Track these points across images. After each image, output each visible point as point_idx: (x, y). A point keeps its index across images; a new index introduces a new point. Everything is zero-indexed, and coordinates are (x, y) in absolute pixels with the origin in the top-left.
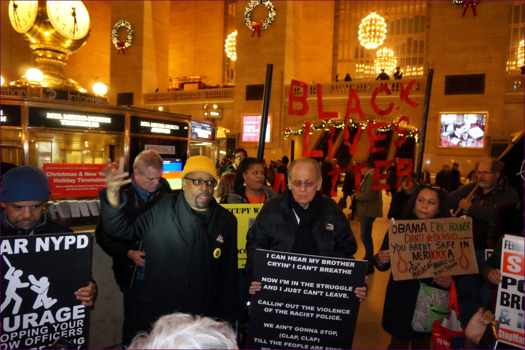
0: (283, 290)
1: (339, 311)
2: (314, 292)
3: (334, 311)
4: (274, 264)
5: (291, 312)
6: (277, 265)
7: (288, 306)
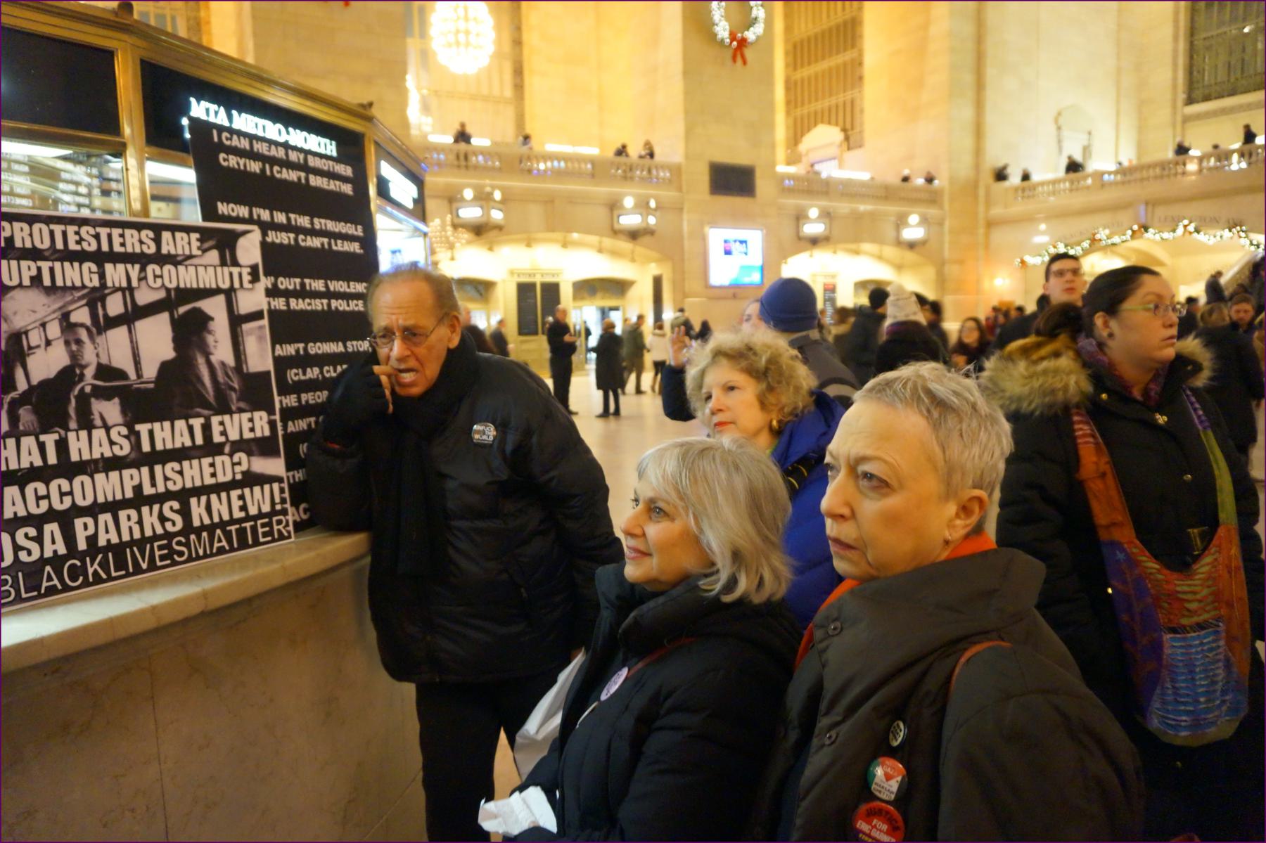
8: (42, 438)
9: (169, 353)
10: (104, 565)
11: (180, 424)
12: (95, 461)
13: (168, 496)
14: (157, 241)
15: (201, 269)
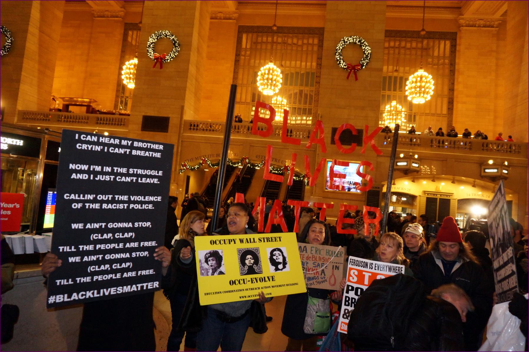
0: (94, 177)
1: (152, 199)
3: (147, 199)
4: (84, 147)
5: (104, 205)
6: (88, 148)
7: (100, 197)
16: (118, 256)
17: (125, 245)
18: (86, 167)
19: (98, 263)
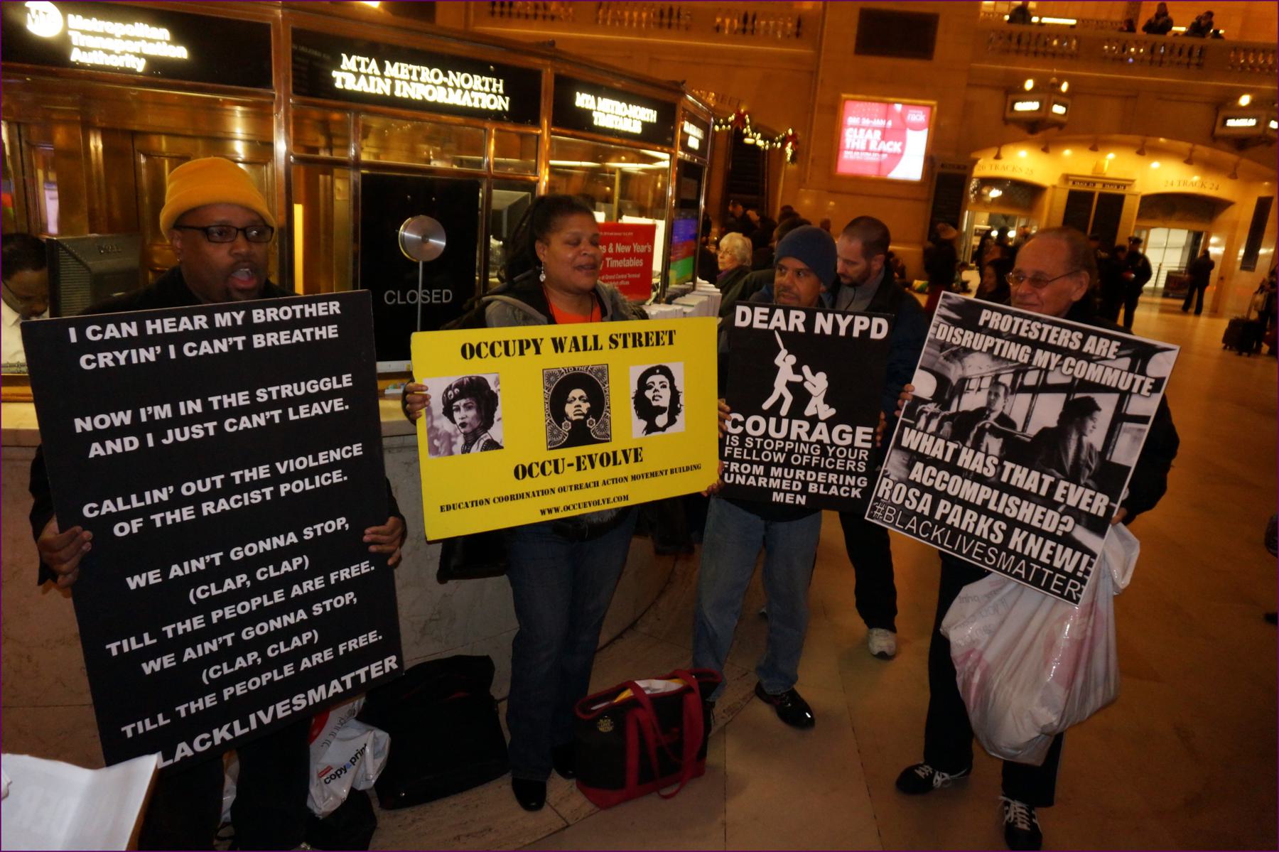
0: (157, 440)
1: (335, 455)
2: (255, 417)
4: (105, 359)
5: (204, 505)
6: (115, 360)
8: (949, 444)
9: (1052, 422)
10: (943, 535)
11: (1035, 475)
12: (970, 472)
13: (1002, 517)
14: (1083, 342)
15: (1109, 370)
16: (275, 624)
17: (287, 593)
18: (125, 418)
19: (226, 654)
